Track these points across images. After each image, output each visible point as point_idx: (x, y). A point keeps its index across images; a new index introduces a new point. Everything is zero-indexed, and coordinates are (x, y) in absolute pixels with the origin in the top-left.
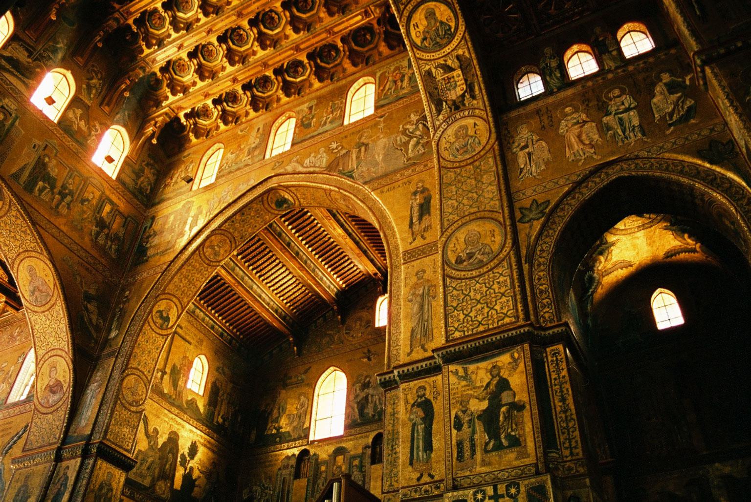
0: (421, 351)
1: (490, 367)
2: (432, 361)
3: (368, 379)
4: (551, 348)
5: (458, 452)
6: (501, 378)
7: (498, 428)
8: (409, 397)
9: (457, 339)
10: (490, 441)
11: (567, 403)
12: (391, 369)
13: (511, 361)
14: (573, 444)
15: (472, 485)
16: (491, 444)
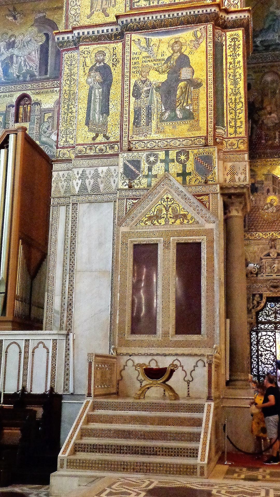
0: (102, 15)
1: (172, 42)
2: (114, 27)
3: (13, 39)
4: (231, 33)
5: (135, 119)
6: (182, 54)
7: (175, 101)
8: (88, 60)
9: (142, 8)
10: (165, 112)
11: (238, 86)
12: (70, 29)
13: (194, 39)
14: (238, 124)
15: (145, 148)
16: (167, 114)
